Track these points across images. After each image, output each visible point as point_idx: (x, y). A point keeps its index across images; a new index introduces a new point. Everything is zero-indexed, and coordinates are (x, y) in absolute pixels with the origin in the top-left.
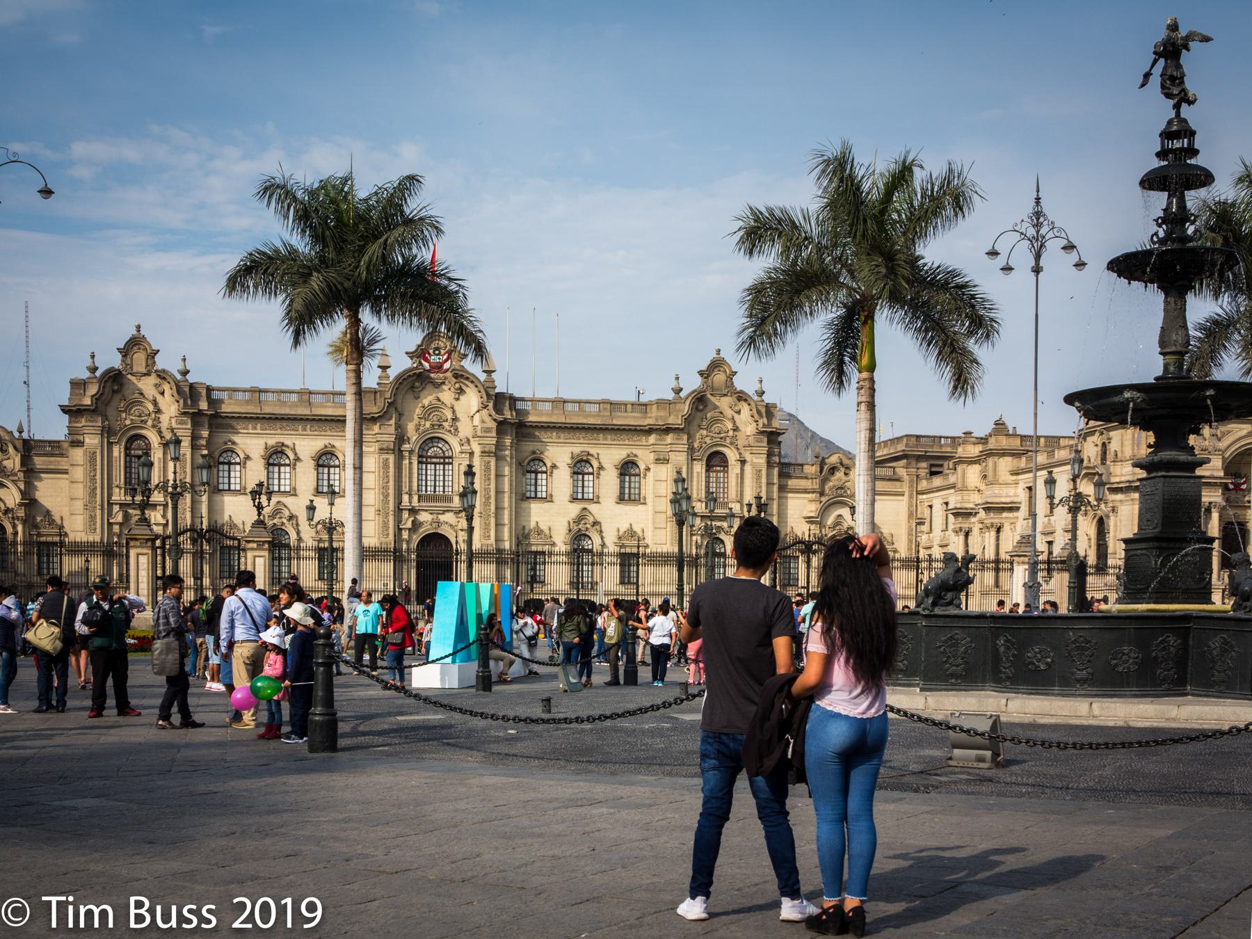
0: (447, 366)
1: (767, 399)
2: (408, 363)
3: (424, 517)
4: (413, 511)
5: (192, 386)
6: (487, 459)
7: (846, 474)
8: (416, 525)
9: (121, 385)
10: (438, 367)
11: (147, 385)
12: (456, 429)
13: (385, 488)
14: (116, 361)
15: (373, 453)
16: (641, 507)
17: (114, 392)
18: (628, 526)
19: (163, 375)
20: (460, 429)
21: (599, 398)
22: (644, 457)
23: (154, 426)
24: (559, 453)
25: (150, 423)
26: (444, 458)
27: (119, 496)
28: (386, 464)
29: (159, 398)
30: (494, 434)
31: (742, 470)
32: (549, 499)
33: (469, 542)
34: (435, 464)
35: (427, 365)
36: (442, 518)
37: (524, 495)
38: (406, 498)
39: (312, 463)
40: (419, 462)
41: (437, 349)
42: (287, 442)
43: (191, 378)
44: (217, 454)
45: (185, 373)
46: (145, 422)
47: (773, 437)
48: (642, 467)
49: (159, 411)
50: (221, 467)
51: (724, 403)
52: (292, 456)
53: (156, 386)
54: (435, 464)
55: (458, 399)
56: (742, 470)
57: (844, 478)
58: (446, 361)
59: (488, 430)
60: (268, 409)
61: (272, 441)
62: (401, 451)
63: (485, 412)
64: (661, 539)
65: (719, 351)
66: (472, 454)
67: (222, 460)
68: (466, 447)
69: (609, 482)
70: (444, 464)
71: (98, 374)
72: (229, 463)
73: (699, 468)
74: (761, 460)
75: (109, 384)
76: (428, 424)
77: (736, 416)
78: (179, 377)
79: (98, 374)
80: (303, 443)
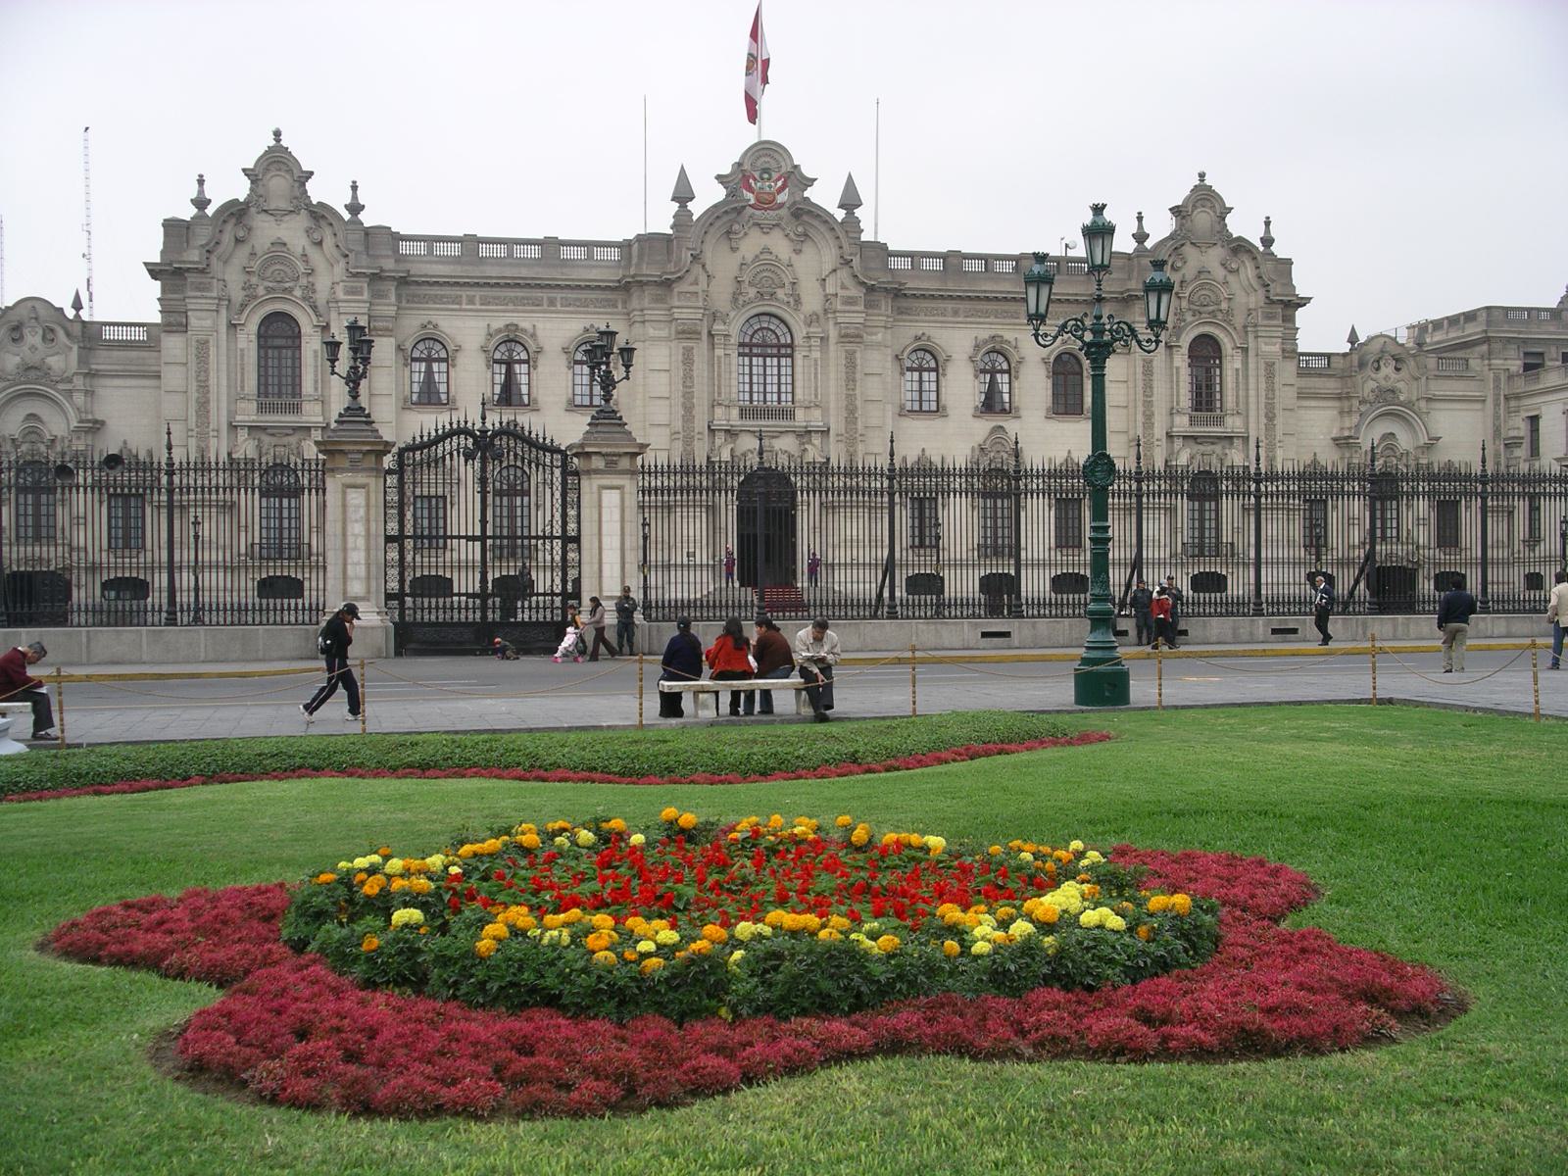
0: (782, 198)
1: (1279, 250)
4: (731, 433)
5: (368, 232)
6: (849, 347)
7: (1397, 369)
10: (766, 203)
11: (293, 233)
12: (798, 301)
13: (688, 396)
14: (241, 190)
15: (668, 339)
17: (238, 241)
19: (321, 214)
20: (804, 299)
21: (1017, 252)
23: (304, 299)
25: (298, 293)
26: (779, 346)
27: (248, 413)
28: (688, 359)
29: (315, 255)
30: (862, 308)
31: (1245, 363)
32: (939, 411)
35: (751, 198)
37: (902, 407)
39: (563, 360)
40: (740, 355)
41: (766, 170)
43: (368, 219)
44: (409, 345)
45: (355, 208)
46: (289, 291)
47: (1288, 312)
49: (311, 272)
51: (1214, 258)
52: (532, 348)
53: (308, 232)
54: (765, 356)
55: (798, 252)
56: (1245, 363)
57: (1394, 376)
58: (781, 190)
59: (850, 301)
60: (492, 271)
61: (498, 323)
63: (844, 274)
65: (1202, 176)
66: (824, 340)
67: (416, 354)
69: (1033, 386)
70: (779, 356)
71: (210, 211)
72: (429, 360)
74: (1276, 348)
75: (229, 227)
76: (752, 292)
77: (1231, 278)
78: (347, 216)
79: (210, 211)
80: (548, 325)
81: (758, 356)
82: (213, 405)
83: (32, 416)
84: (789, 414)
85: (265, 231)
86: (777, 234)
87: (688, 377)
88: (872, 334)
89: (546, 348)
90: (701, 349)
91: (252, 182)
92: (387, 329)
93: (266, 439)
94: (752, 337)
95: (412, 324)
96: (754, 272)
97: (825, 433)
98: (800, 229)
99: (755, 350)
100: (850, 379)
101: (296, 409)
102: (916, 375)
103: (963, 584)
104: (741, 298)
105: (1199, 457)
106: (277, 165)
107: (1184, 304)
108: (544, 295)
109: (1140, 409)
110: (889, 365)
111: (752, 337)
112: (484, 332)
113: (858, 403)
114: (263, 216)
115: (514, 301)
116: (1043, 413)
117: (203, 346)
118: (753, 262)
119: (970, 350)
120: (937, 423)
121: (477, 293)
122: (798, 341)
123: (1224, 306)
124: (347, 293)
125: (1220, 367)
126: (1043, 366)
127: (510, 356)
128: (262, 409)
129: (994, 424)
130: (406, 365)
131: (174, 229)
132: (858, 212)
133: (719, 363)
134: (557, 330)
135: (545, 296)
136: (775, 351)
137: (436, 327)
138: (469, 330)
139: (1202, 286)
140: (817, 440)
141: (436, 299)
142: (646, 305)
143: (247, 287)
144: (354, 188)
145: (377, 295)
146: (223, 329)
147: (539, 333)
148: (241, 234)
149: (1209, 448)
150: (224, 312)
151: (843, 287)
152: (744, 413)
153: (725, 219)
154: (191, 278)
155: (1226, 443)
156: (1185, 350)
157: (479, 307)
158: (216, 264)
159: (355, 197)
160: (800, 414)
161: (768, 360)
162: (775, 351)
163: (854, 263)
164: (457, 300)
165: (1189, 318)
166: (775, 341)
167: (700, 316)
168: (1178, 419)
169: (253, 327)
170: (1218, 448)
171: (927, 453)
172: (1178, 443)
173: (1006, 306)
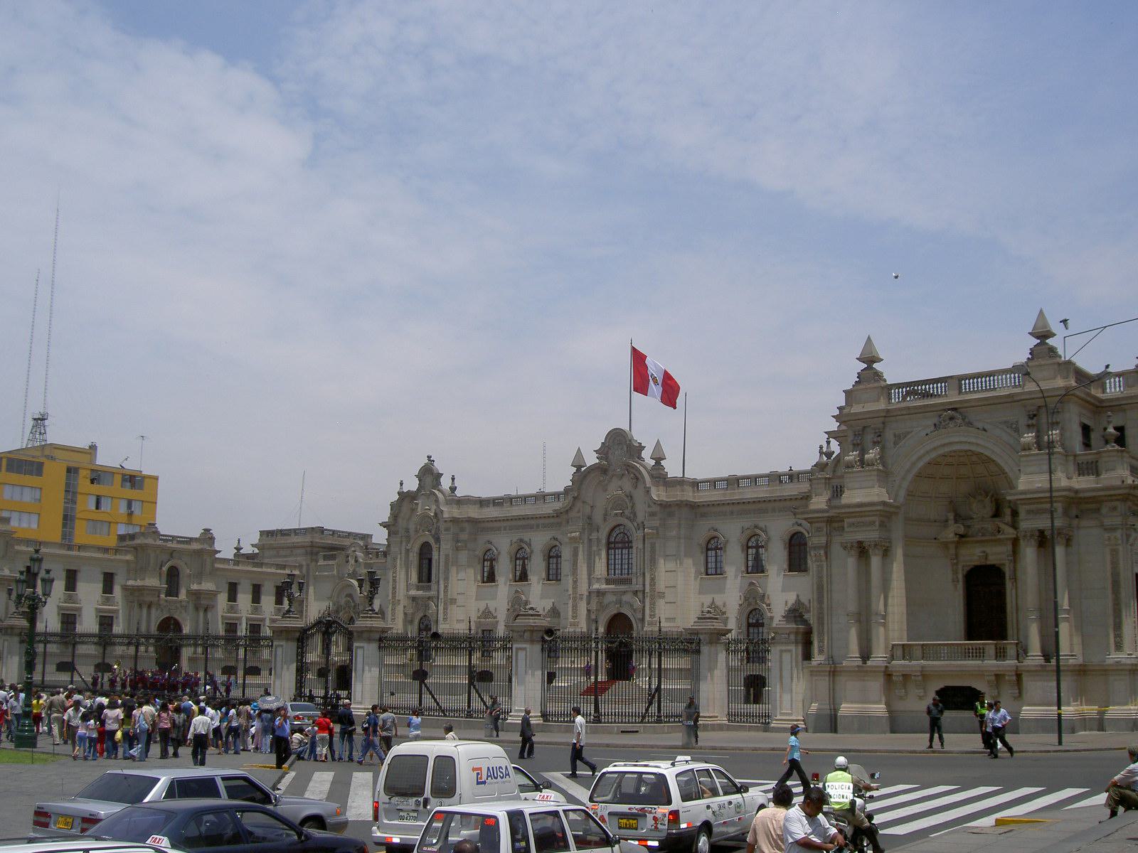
2: (597, 461)
3: (610, 598)
4: (600, 593)
8: (602, 607)
12: (635, 515)
24: (732, 531)
25: (433, 532)
36: (625, 598)
40: (608, 549)
42: (526, 539)
43: (459, 493)
44: (480, 553)
45: (453, 489)
59: (652, 514)
61: (515, 540)
62: (590, 540)
69: (776, 556)
81: (618, 548)
89: (535, 550)
97: (644, 591)
99: (617, 546)
101: (429, 589)
102: (713, 552)
106: (429, 474)
110: (682, 548)
124: (445, 530)
127: (757, 544)
131: (392, 505)
132: (663, 463)
134: (539, 541)
137: (490, 543)
138: (503, 544)
140: (640, 595)
143: (417, 531)
144: (453, 479)
145: (462, 530)
146: (403, 552)
147: (532, 543)
150: (404, 544)
161: (624, 550)
164: (499, 529)
169: (416, 549)
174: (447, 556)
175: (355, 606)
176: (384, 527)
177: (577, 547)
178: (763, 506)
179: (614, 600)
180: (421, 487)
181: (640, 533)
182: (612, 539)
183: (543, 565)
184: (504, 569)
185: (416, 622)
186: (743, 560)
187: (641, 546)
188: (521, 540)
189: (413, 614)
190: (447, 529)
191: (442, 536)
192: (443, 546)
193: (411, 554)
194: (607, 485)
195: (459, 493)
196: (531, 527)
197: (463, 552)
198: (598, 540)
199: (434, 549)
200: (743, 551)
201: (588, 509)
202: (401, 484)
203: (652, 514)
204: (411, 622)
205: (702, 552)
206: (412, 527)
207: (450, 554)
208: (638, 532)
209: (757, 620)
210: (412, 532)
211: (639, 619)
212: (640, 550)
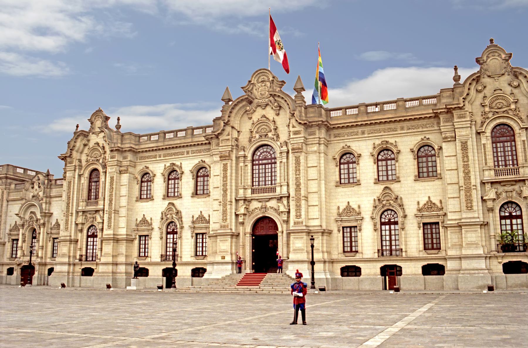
3: (255, 205)
5: (122, 135)
9: (89, 141)
12: (278, 136)
16: (437, 182)
18: (427, 199)
20: (280, 136)
22: (434, 139)
25: (101, 161)
26: (271, 159)
28: (225, 170)
29: (105, 145)
33: (287, 222)
34: (265, 164)
38: (241, 192)
40: (253, 165)
42: (178, 163)
43: (122, 130)
45: (118, 127)
48: (436, 147)
49: (105, 153)
50: (143, 184)
51: (503, 82)
53: (104, 137)
55: (278, 115)
59: (296, 133)
61: (168, 164)
63: (293, 121)
64: (454, 210)
66: (288, 153)
68: (285, 148)
69: (407, 164)
70: (271, 164)
73: (486, 140)
76: (257, 136)
77: (516, 91)
81: (262, 164)
82: (71, 205)
83: (31, 212)
84: (274, 190)
85: (94, 139)
86: (268, 108)
87: (225, 177)
88: (311, 147)
89: (185, 172)
90: (231, 164)
91: (92, 123)
92: (125, 170)
93: (89, 216)
94: (259, 156)
95: (140, 167)
96: (258, 126)
97: (288, 197)
98: (276, 104)
99: (260, 162)
100: (297, 169)
103: (371, 271)
104: (253, 139)
105: (504, 194)
107: (487, 109)
108: (185, 150)
109: (461, 169)
110: (322, 161)
111: (259, 156)
112: (163, 168)
113: (302, 181)
114: (94, 135)
115: (174, 154)
116: (413, 178)
117: (70, 183)
118: (258, 121)
119: (371, 150)
120: (356, 188)
121: (162, 153)
122: (278, 155)
123: (513, 106)
124: (111, 158)
125: (515, 141)
126: (411, 153)
128: (87, 205)
129: (383, 187)
130: (137, 184)
133: (241, 169)
134: (188, 164)
135: (185, 151)
136: (270, 161)
137: (147, 168)
138: (158, 169)
139: (497, 97)
140: (285, 201)
141: (148, 157)
142: (214, 148)
143: (87, 161)
146: (77, 176)
147: (183, 166)
148: (84, 142)
149: (509, 188)
150: (77, 171)
151: (293, 127)
152: (253, 192)
153: (241, 105)
154: (68, 159)
155: (521, 184)
156: (488, 134)
157: (162, 158)
158: (75, 154)
159: (118, 122)
160: (278, 189)
162: (270, 161)
163: (295, 115)
165: (490, 115)
166: (270, 157)
167: (230, 149)
168: (486, 173)
169: (87, 174)
170: (516, 187)
171: (350, 204)
172: (488, 186)
173: (387, 126)
174: (112, 178)
175: (37, 220)
176: (62, 159)
177: (227, 164)
178: (392, 126)
179: (260, 206)
180: (92, 128)
181: (285, 148)
182: (256, 157)
183: (192, 183)
184: (158, 187)
185: (85, 232)
186: (376, 170)
187: (285, 160)
188: (174, 164)
189: (83, 224)
190: (112, 157)
191: (108, 164)
192: (109, 170)
193: (82, 179)
194: (252, 113)
195: (122, 130)
196: (182, 154)
197: (126, 174)
198: (245, 157)
199: (101, 174)
200: (375, 163)
201: (235, 135)
202: (77, 126)
203: (296, 133)
204: (81, 231)
205: (337, 166)
206: (84, 158)
207: (115, 176)
208: (282, 149)
209: (390, 220)
210: (84, 163)
211: (284, 221)
212: (284, 163)
